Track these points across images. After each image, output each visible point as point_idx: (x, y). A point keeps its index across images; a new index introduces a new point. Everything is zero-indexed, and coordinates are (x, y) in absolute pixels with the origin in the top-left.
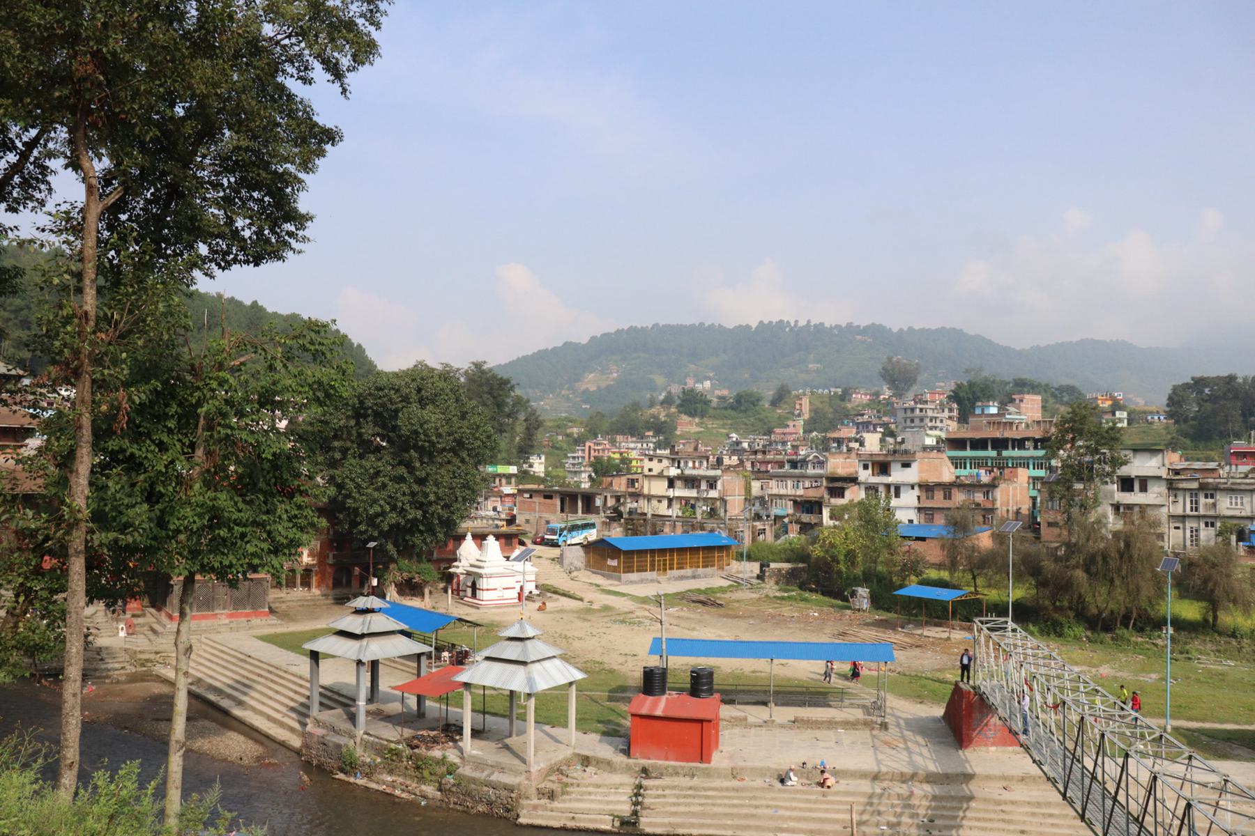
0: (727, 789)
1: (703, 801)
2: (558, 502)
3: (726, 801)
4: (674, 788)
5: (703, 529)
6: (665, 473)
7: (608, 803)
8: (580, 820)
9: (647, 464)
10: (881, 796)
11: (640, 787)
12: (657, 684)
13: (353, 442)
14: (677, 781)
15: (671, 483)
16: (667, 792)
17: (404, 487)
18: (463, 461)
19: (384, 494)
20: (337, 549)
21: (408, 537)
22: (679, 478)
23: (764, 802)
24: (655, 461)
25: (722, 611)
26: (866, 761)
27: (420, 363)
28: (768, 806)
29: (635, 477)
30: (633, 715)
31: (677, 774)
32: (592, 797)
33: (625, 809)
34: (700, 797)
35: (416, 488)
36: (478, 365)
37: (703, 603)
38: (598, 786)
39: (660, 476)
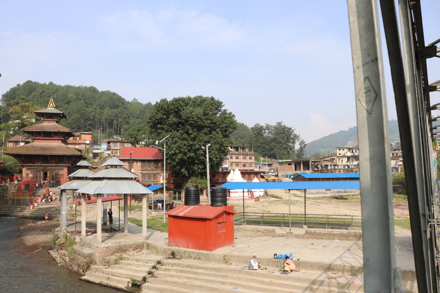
0: (211, 269)
1: (191, 276)
2: (293, 166)
3: (206, 277)
4: (178, 265)
5: (352, 172)
6: (346, 155)
7: (135, 271)
8: (112, 280)
9: (338, 152)
10: (322, 283)
11: (159, 263)
12: (193, 196)
13: (167, 125)
14: (190, 262)
15: (348, 158)
16: (174, 267)
17: (185, 142)
18: (218, 133)
19: (176, 146)
20: (175, 177)
21: (192, 167)
22: (352, 157)
23: (231, 281)
24: (342, 150)
25: (346, 201)
26: (327, 258)
27: (257, 124)
28: (231, 284)
29: (333, 157)
30: (169, 216)
31: (190, 257)
32: (131, 267)
33: (139, 276)
34: (190, 272)
35: (191, 143)
36: (279, 124)
37: (337, 198)
38: (138, 261)
39: (344, 156)
